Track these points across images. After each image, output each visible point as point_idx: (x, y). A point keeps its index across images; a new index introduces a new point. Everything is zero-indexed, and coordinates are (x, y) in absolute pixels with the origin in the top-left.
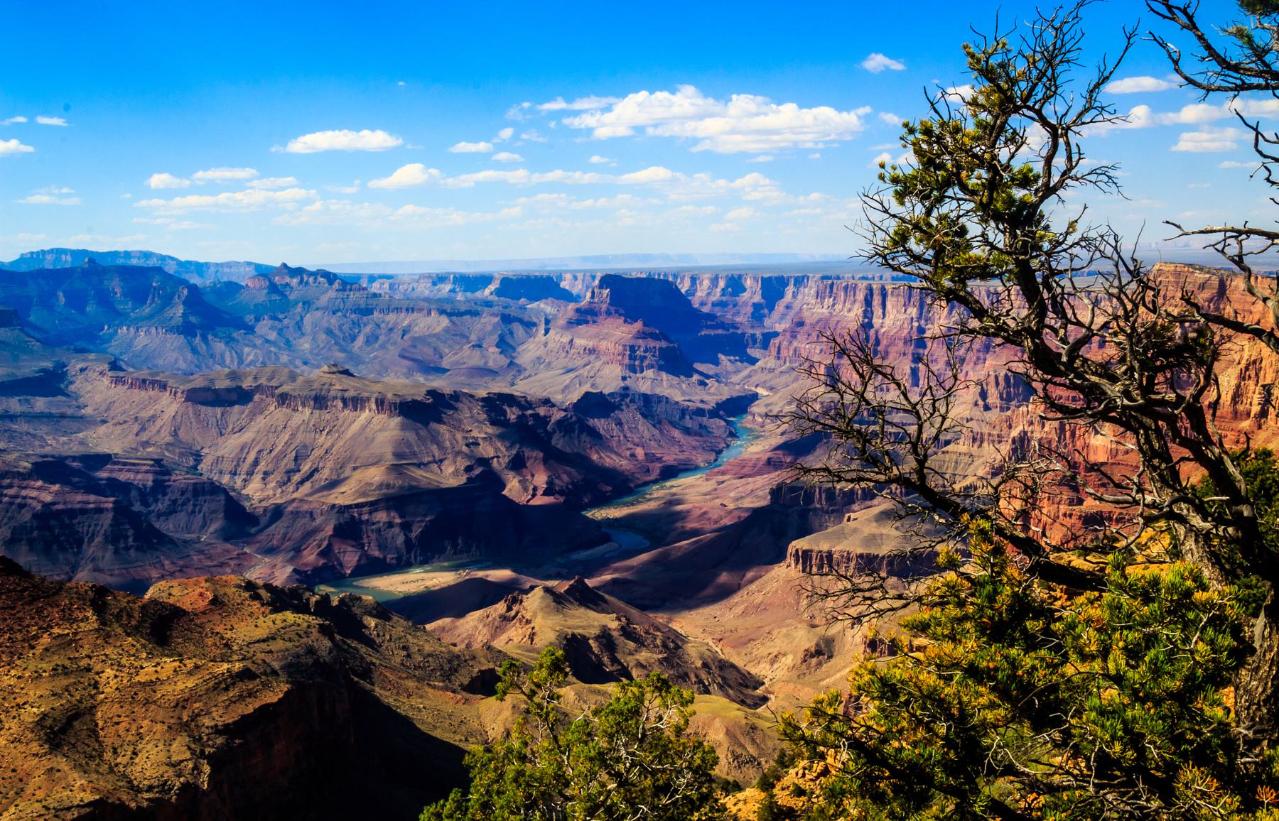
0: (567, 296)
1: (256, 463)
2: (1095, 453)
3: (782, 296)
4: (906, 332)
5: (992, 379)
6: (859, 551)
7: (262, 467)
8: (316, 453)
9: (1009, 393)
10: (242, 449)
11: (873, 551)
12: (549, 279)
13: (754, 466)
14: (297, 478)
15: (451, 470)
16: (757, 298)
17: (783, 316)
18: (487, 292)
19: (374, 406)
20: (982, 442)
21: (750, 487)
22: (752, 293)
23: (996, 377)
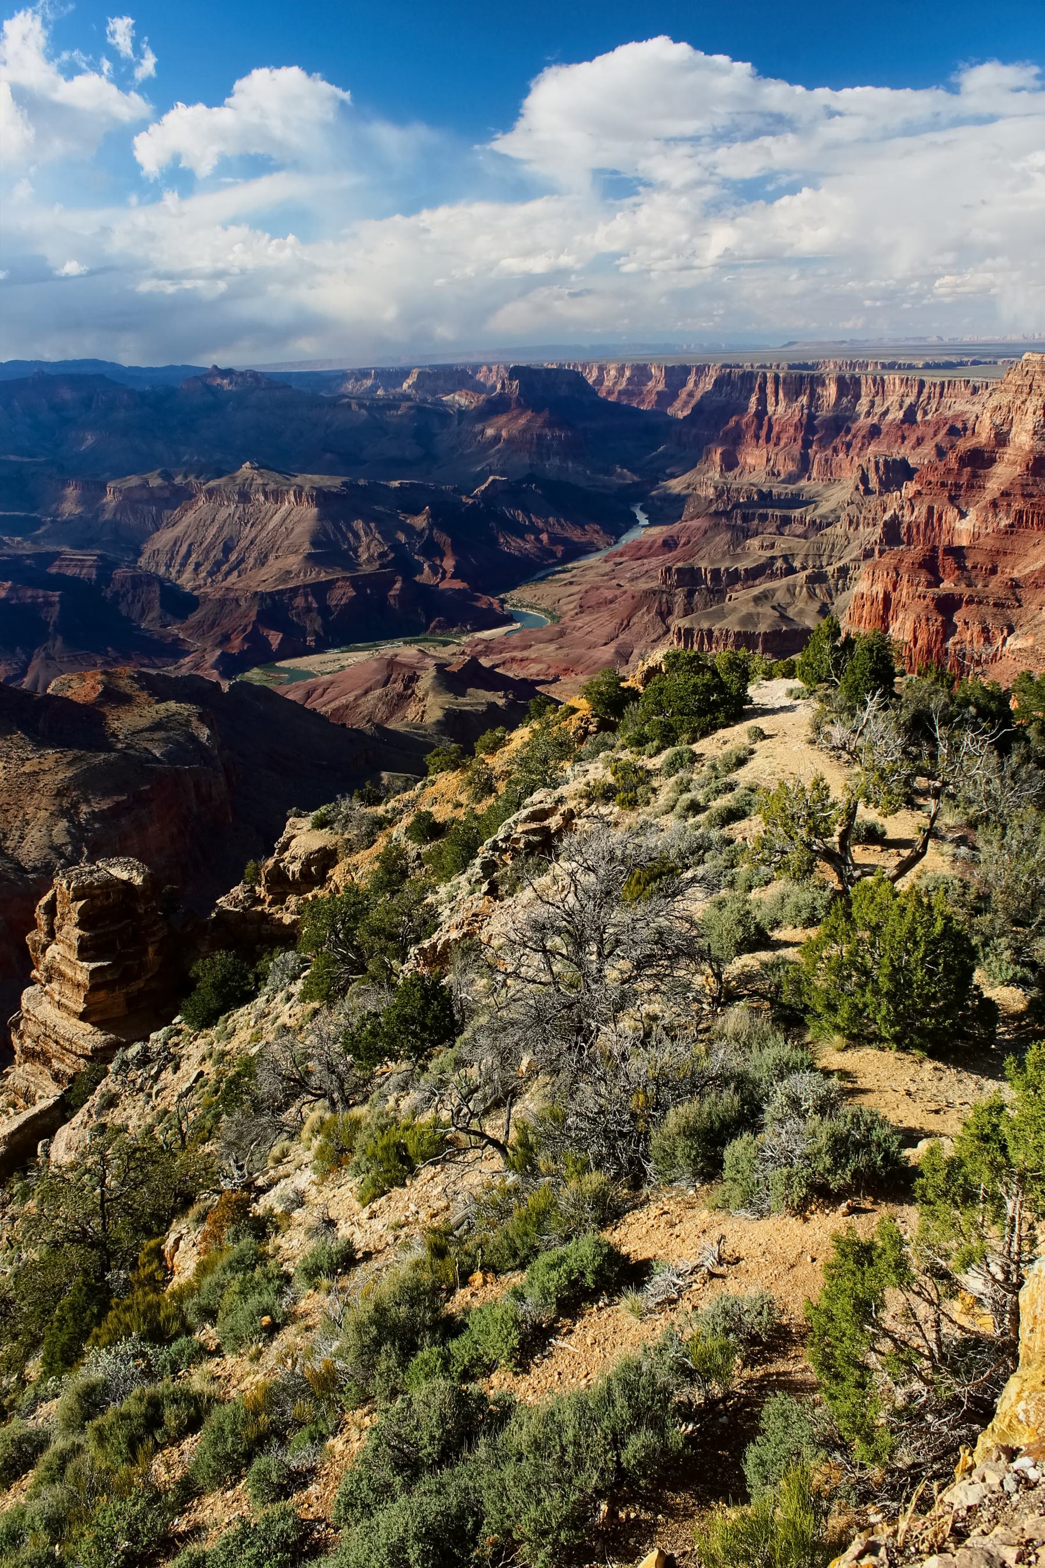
0: (479, 388)
1: (189, 554)
2: (959, 536)
3: (684, 384)
4: (797, 418)
5: (872, 464)
6: (737, 629)
7: (194, 558)
8: (243, 544)
9: (887, 477)
10: (175, 543)
11: (750, 629)
12: (464, 372)
13: (650, 548)
14: (225, 568)
15: (365, 556)
16: (661, 387)
17: (686, 403)
18: (405, 386)
19: (293, 499)
20: (858, 525)
21: (645, 568)
22: (657, 384)
23: (877, 463)
